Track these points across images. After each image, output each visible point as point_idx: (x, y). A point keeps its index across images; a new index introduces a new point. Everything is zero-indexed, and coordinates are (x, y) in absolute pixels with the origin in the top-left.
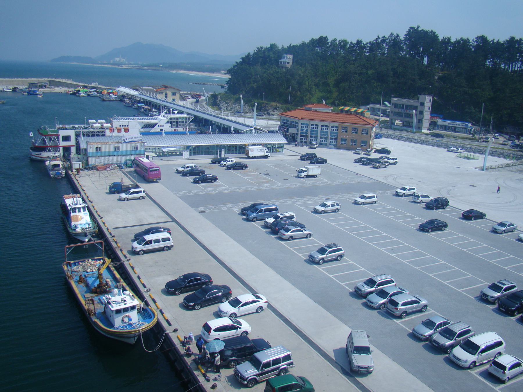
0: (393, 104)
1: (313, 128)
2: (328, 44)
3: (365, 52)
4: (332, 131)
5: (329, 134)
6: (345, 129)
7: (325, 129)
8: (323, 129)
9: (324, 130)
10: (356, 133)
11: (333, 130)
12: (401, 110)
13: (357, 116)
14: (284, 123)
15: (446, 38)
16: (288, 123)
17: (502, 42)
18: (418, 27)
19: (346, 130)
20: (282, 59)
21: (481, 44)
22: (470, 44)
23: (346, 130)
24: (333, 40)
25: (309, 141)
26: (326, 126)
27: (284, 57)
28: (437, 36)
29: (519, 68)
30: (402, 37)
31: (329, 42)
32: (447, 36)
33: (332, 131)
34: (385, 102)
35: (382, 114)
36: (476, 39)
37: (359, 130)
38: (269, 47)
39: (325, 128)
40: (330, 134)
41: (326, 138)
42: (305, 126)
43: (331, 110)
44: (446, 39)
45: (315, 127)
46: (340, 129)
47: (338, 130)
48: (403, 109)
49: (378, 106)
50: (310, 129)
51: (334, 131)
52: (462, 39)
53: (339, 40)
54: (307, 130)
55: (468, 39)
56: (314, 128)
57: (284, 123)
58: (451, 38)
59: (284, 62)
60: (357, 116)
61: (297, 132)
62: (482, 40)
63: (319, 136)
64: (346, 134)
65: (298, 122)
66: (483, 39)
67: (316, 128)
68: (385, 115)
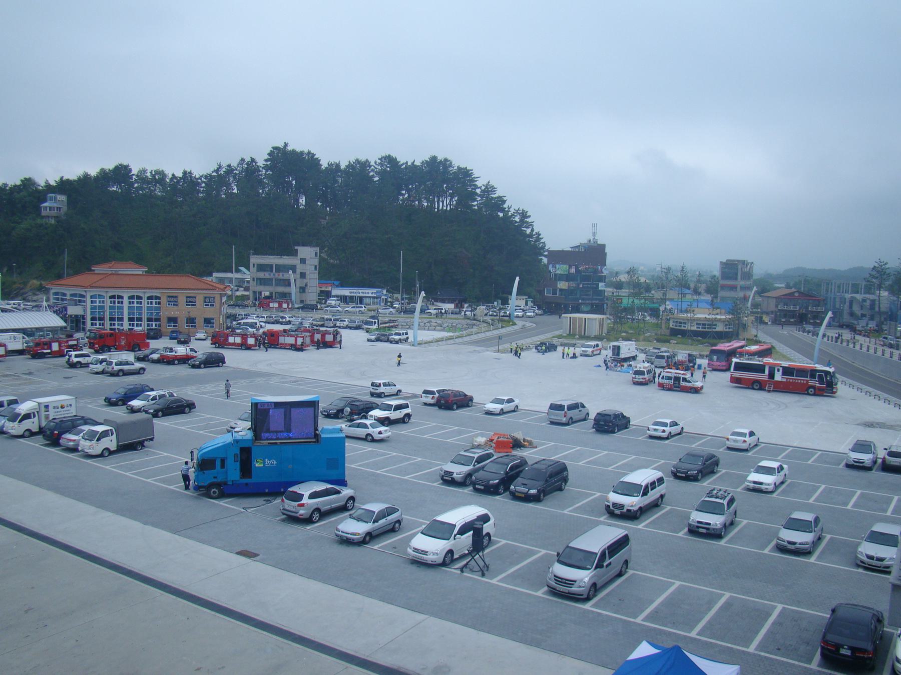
0: (254, 265)
1: (114, 303)
2: (132, 178)
3: (199, 192)
4: (149, 305)
6: (173, 300)
7: (135, 302)
8: (133, 303)
10: (192, 305)
11: (152, 303)
12: (270, 275)
14: (58, 299)
15: (333, 163)
16: (66, 300)
17: (420, 164)
18: (286, 145)
20: (45, 201)
21: (388, 169)
22: (372, 167)
24: (140, 171)
27: (51, 199)
28: (317, 161)
29: (449, 206)
30: (261, 163)
31: (133, 175)
32: (334, 160)
34: (240, 268)
35: (236, 286)
36: (379, 161)
38: (21, 185)
39: (135, 301)
40: (146, 311)
41: (140, 319)
43: (146, 272)
44: (333, 164)
45: (116, 300)
46: (164, 300)
47: (160, 303)
49: (229, 275)
50: (108, 303)
51: (154, 305)
52: (358, 161)
53: (152, 171)
54: (102, 307)
55: (367, 161)
56: (116, 302)
57: (58, 299)
58: (341, 164)
59: (50, 208)
61: (84, 311)
62: (389, 163)
64: (175, 308)
65: (84, 293)
66: (390, 160)
68: (243, 289)
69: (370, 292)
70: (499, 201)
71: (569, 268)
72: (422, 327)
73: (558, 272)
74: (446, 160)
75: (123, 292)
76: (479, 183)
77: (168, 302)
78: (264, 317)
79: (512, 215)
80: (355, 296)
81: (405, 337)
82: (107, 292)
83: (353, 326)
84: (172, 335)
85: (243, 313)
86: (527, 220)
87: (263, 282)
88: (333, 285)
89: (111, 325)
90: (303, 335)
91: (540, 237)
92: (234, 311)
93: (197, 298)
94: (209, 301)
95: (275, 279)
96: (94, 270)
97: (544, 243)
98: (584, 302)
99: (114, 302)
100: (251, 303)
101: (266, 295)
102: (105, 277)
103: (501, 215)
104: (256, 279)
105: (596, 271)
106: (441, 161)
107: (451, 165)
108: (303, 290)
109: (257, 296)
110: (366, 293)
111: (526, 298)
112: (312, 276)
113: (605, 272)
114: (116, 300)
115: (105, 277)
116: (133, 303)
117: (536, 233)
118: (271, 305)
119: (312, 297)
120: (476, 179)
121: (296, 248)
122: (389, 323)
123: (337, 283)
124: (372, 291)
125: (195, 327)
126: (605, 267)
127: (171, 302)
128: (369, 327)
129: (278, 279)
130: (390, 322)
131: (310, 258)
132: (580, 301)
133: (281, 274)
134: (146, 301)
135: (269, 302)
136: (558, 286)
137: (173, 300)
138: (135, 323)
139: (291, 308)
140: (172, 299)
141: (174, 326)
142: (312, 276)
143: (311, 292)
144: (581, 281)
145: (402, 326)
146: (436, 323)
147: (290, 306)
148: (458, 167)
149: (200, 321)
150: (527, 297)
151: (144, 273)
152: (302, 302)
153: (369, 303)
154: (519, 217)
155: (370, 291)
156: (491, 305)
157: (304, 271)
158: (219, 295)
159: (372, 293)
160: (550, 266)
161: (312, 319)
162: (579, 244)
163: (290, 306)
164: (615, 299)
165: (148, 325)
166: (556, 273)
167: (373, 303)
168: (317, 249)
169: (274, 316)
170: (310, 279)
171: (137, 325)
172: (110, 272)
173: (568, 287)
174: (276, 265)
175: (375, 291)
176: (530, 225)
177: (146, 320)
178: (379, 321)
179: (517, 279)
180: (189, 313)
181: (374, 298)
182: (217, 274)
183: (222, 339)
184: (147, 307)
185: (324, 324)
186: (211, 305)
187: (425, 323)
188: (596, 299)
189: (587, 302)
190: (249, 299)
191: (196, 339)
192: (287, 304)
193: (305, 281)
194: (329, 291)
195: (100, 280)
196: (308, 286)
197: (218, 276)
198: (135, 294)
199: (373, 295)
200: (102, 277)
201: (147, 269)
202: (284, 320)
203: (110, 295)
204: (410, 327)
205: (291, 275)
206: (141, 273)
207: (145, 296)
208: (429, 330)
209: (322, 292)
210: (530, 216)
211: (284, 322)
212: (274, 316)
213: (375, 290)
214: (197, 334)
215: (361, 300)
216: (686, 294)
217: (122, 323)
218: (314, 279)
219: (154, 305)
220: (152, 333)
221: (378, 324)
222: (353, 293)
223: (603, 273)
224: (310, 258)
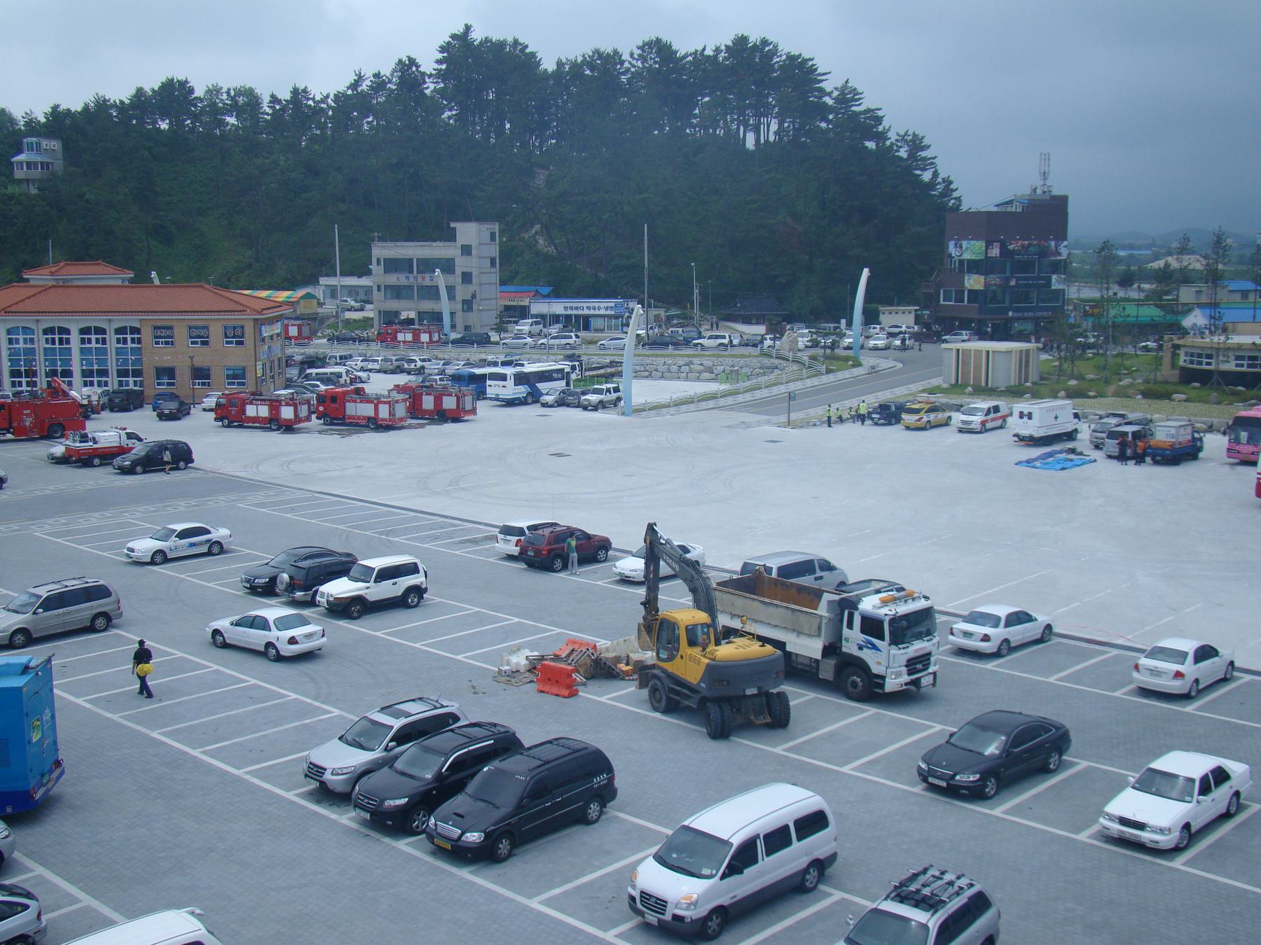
0: (378, 260)
1: (54, 343)
4: (121, 346)
6: (164, 334)
7: (93, 341)
8: (90, 341)
9: (94, 345)
11: (125, 341)
12: (407, 278)
13: (207, 289)
17: (711, 53)
33: (121, 346)
35: (361, 301)
37: (211, 334)
39: (93, 337)
41: (103, 373)
42: (21, 337)
43: (131, 281)
46: (147, 334)
47: (139, 341)
48: (411, 271)
50: (41, 343)
51: (130, 345)
60: (207, 289)
63: (76, 368)
64: (169, 348)
69: (602, 306)
70: (868, 118)
71: (987, 247)
72: (646, 373)
73: (966, 256)
74: (765, 42)
76: (827, 86)
77: (156, 337)
78: (377, 361)
79: (892, 144)
80: (577, 316)
82: (38, 321)
84: (156, 403)
85: (338, 355)
86: (923, 154)
87: (397, 292)
88: (538, 295)
91: (952, 187)
93: (211, 329)
94: (235, 336)
96: (27, 280)
97: (958, 199)
98: (1020, 314)
99: (53, 339)
100: (376, 333)
101: (410, 317)
102: (39, 293)
103: (871, 145)
104: (383, 289)
105: (1044, 253)
106: (755, 44)
107: (775, 51)
108: (468, 305)
109: (390, 318)
110: (594, 308)
111: (916, 310)
112: (485, 279)
113: (1064, 253)
115: (39, 293)
116: (90, 341)
117: (943, 179)
118: (400, 337)
119: (483, 319)
120: (820, 78)
121: (452, 225)
122: (613, 367)
123: (546, 290)
124: (606, 305)
125: (209, 386)
126: (1066, 243)
127: (160, 337)
130: (612, 364)
131: (480, 244)
132: (1010, 314)
133: (427, 276)
134: (115, 337)
135: (396, 332)
136: (967, 284)
137: (164, 334)
138: (95, 380)
139: (437, 342)
141: (169, 384)
142: (485, 279)
143: (481, 310)
144: (1012, 272)
145: (636, 372)
146: (702, 365)
147: (436, 337)
148: (791, 58)
149: (218, 375)
150: (918, 308)
151: (127, 283)
152: (467, 328)
153: (602, 327)
154: (906, 149)
155: (602, 305)
156: (832, 325)
157: (468, 270)
159: (607, 309)
160: (951, 245)
161: (462, 363)
162: (1012, 198)
163: (436, 337)
164: (1087, 308)
165: (121, 384)
166: (963, 258)
167: (610, 328)
168: (496, 227)
171: (100, 384)
172: (54, 283)
173: (985, 286)
175: (613, 305)
176: (927, 163)
177: (115, 373)
178: (581, 364)
179: (866, 272)
180: (192, 358)
181: (609, 317)
183: (234, 410)
184: (117, 348)
188: (1042, 309)
189: (1026, 314)
190: (372, 326)
192: (428, 335)
193: (472, 288)
194: (525, 306)
195: (29, 298)
196: (478, 299)
197: (329, 283)
198: (93, 325)
200: (33, 293)
202: (412, 366)
203: (44, 327)
204: (650, 375)
205: (440, 280)
206: (119, 283)
208: (687, 379)
209: (507, 308)
210: (928, 147)
212: (394, 358)
213: (611, 303)
214: (204, 400)
215: (584, 323)
216: (1249, 291)
217: (71, 381)
218: (490, 284)
219: (130, 345)
220: (117, 401)
221: (581, 370)
222: (571, 308)
223: (1059, 254)
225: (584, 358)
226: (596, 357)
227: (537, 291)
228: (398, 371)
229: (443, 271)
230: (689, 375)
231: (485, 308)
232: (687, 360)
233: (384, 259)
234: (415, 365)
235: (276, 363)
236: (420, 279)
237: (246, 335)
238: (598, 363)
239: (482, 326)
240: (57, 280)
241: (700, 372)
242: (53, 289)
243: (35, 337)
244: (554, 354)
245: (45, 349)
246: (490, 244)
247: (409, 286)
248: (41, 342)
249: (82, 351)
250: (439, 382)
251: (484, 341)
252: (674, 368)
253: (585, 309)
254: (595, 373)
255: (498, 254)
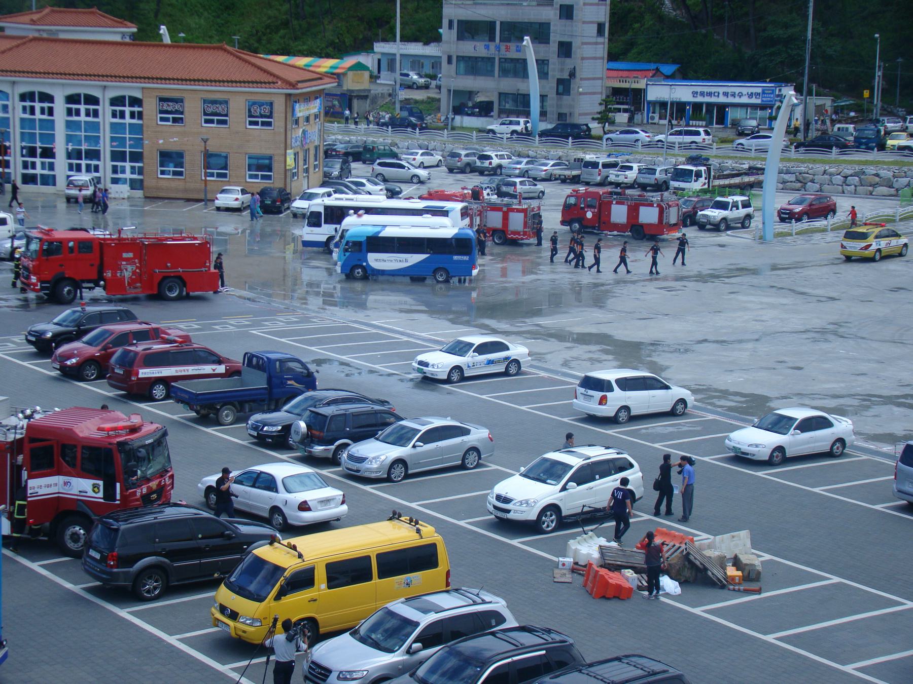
0: (451, 23)
5: (106, 135)
7: (83, 112)
8: (78, 113)
9: (83, 118)
10: (219, 122)
11: (122, 115)
12: (487, 47)
19: (177, 112)
23: (177, 112)
25: (21, 171)
26: (92, 100)
35: (427, 76)
37: (231, 111)
39: (82, 108)
41: (94, 154)
43: (133, 36)
46: (150, 107)
47: (140, 115)
48: (492, 39)
51: (128, 120)
56: (38, 111)
63: (60, 147)
64: (178, 127)
67: (43, 112)
75: (53, 84)
77: (162, 112)
80: (710, 106)
81: (742, 212)
82: (14, 83)
83: (646, 181)
87: (473, 66)
89: (25, 165)
90: (525, 207)
92: (381, 140)
93: (232, 105)
95: (500, 59)
108: (564, 86)
110: (733, 95)
112: (588, 51)
114: (38, 106)
115: (18, 46)
116: (78, 113)
122: (752, 174)
123: (668, 69)
128: (682, 185)
129: (506, 60)
130: (753, 171)
131: (585, 4)
133: (513, 46)
134: (109, 109)
138: (83, 163)
140: (171, 106)
141: (175, 173)
142: (588, 51)
143: (581, 94)
149: (238, 164)
151: (127, 40)
152: (561, 116)
155: (745, 91)
157: (566, 39)
158: (282, 99)
159: (750, 95)
161: (552, 163)
169: (463, 153)
170: (583, 59)
172: (36, 35)
174: (501, 23)
175: (759, 90)
178: (709, 170)
181: (754, 107)
182: (382, 44)
184: (112, 124)
185: (578, 176)
186: (264, 124)
187: (846, 177)
191: (218, 209)
193: (569, 63)
194: (640, 90)
198: (83, 91)
199: (754, 101)
200: (9, 46)
201: (135, 30)
202: (486, 163)
206: (118, 38)
207: (105, 98)
209: (616, 92)
211: (487, 169)
212: (463, 153)
213: (756, 88)
214: (219, 196)
218: (595, 58)
219: (128, 120)
221: (708, 177)
222: (702, 94)
224: (585, 4)
225: (714, 162)
226: (730, 162)
227: (657, 70)
228: (468, 170)
229: (534, 40)
230: (858, 188)
231: (586, 91)
232: (857, 168)
233: (458, 21)
234: (490, 163)
235: (312, 152)
236: (503, 48)
237: (275, 115)
238: (733, 169)
239: (580, 115)
240: (39, 30)
241: (874, 185)
242: (33, 44)
243: (9, 103)
244: (674, 155)
245: (22, 120)
246: (597, 5)
247: (489, 59)
248: (16, 111)
249: (69, 125)
250: (518, 186)
251: (581, 134)
252: (839, 179)
253: (721, 95)
254: (727, 182)
255: (608, 20)
